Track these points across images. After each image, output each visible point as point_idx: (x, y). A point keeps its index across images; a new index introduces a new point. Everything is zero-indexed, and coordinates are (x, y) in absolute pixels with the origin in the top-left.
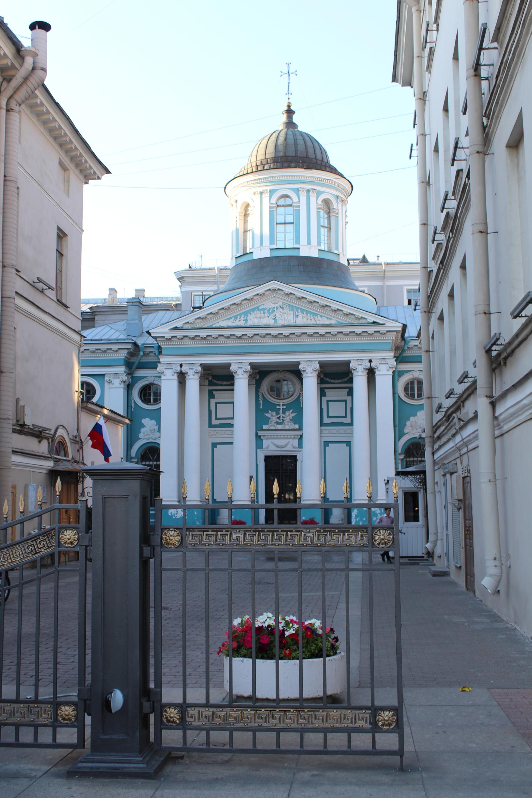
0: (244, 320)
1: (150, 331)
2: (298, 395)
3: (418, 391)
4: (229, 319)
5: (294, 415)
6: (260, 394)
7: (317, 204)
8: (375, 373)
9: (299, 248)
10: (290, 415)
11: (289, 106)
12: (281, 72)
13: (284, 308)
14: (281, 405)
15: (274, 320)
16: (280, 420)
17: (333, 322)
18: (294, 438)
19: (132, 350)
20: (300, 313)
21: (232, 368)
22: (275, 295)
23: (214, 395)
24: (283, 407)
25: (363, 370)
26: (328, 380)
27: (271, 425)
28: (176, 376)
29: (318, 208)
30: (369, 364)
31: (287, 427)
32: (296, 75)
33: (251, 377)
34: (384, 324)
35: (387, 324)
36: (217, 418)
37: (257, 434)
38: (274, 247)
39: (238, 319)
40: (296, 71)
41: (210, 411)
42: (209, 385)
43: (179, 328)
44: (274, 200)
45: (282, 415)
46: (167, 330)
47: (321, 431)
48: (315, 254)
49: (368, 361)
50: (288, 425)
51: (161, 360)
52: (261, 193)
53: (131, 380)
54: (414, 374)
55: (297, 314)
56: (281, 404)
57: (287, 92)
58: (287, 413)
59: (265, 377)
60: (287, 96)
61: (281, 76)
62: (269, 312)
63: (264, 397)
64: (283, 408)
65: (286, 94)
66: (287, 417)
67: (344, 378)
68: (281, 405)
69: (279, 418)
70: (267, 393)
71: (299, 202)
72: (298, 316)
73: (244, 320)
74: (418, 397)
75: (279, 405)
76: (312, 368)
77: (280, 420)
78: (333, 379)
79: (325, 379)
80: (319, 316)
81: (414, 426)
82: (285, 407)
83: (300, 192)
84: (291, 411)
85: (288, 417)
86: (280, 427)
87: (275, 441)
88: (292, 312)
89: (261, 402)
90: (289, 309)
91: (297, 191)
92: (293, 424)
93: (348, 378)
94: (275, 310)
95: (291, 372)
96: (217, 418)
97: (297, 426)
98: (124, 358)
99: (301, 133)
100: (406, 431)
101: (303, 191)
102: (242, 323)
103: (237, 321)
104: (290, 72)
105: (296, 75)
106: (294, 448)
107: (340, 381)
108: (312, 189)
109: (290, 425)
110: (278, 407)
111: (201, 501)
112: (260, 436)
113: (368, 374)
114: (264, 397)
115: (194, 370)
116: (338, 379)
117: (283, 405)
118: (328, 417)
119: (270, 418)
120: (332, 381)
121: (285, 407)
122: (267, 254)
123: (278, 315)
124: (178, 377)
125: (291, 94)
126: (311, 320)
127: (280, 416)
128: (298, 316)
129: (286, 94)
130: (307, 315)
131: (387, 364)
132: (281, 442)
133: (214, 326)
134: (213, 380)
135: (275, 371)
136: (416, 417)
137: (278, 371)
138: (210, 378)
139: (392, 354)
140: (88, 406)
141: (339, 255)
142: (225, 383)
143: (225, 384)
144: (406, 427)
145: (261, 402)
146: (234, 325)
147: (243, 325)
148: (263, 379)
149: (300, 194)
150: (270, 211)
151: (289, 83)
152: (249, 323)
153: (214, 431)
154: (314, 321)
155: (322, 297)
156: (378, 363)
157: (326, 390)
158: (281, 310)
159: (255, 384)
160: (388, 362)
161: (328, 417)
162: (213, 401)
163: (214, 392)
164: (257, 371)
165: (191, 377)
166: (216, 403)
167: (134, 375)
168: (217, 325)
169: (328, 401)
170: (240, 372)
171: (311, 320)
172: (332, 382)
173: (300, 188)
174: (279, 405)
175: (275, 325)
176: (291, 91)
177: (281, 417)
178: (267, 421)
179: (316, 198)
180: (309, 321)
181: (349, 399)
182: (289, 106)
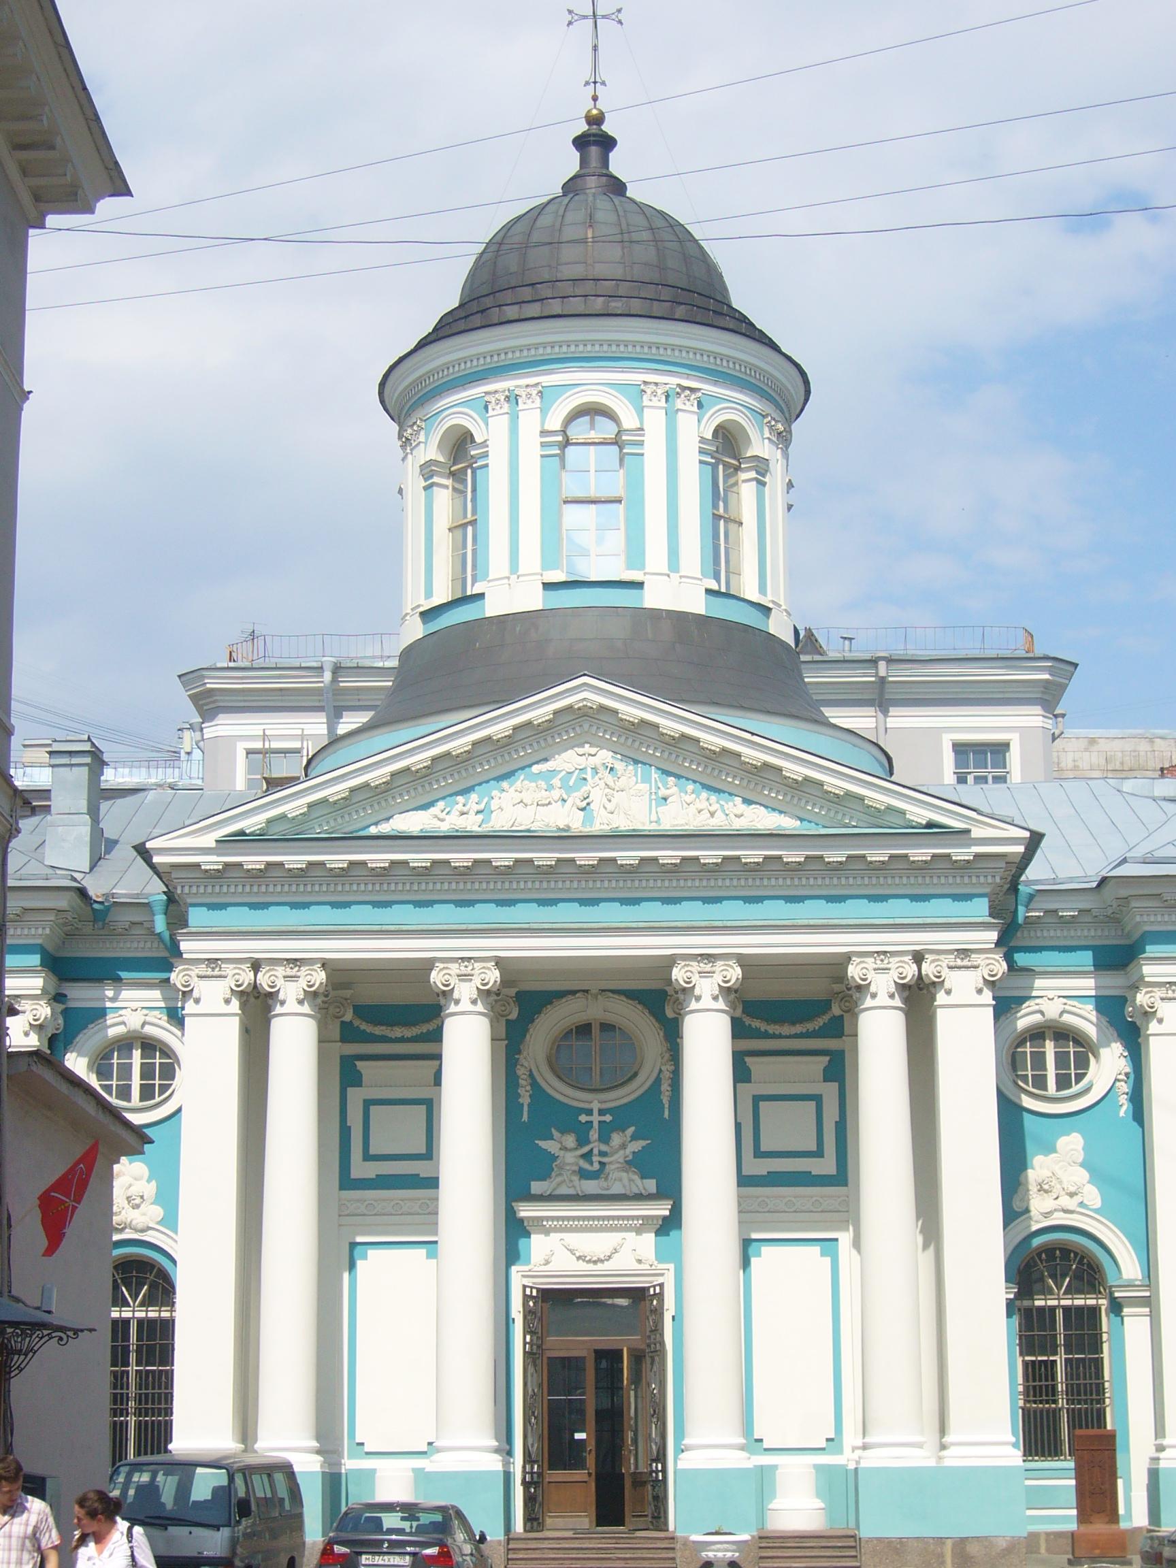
0: (478, 812)
1: (148, 845)
2: (655, 1075)
3: (1058, 1066)
4: (425, 807)
5: (637, 1146)
6: (521, 1071)
7: (703, 440)
8: (933, 998)
9: (639, 585)
10: (626, 1145)
11: (596, 120)
12: (570, 12)
13: (619, 774)
14: (596, 1112)
15: (582, 813)
16: (591, 1164)
17: (787, 823)
18: (639, 1231)
19: (69, 916)
20: (675, 789)
21: (436, 977)
22: (586, 726)
24: (602, 1118)
25: (893, 989)
26: (756, 1024)
27: (559, 1179)
28: (235, 1006)
29: (702, 451)
30: (914, 967)
31: (617, 1189)
32: (620, 22)
33: (496, 1015)
34: (968, 831)
35: (977, 833)
36: (367, 1157)
37: (511, 1214)
38: (558, 576)
39: (460, 807)
40: (619, 11)
41: (345, 1132)
42: (343, 1040)
43: (251, 834)
44: (555, 423)
45: (596, 1147)
46: (209, 840)
47: (739, 1204)
48: (696, 604)
49: (908, 958)
50: (621, 1180)
51: (183, 946)
52: (512, 398)
53: (61, 1021)
54: (1043, 1008)
55: (663, 792)
56: (596, 1106)
57: (587, 75)
58: (616, 1139)
59: (540, 1012)
60: (590, 90)
61: (570, 23)
62: (564, 786)
63: (534, 1084)
64: (599, 1122)
65: (587, 83)
66: (616, 1152)
67: (810, 1018)
68: (596, 1112)
69: (587, 1156)
70: (545, 1069)
71: (642, 429)
72: (665, 799)
73: (478, 812)
74: (1060, 1087)
75: (589, 1112)
76: (718, 978)
77: (591, 1164)
78: (775, 1022)
79: (747, 1021)
80: (738, 800)
81: (1046, 1187)
82: (608, 1118)
83: (645, 397)
84: (632, 1129)
85: (622, 1152)
86: (591, 1187)
87: (573, 1239)
88: (644, 787)
89: (525, 1100)
90: (636, 775)
91: (637, 393)
92: (636, 1178)
93: (826, 1018)
94: (585, 779)
95: (630, 995)
96: (367, 1157)
97: (651, 1185)
98: (39, 941)
99: (642, 208)
101: (654, 394)
102: (471, 824)
103: (455, 812)
104: (599, 12)
105: (620, 22)
106: (639, 1261)
107: (798, 1029)
108: (684, 388)
109: (626, 1181)
110: (583, 1118)
111: (318, 1452)
112: (521, 1220)
113: (906, 1001)
114: (534, 1084)
115: (302, 983)
116: (793, 1023)
117: (602, 1112)
118: (759, 1154)
119: (555, 1158)
120: (771, 1029)
121: (608, 1118)
122: (529, 598)
123: (597, 796)
124: (243, 1006)
125: (603, 83)
126: (712, 814)
127: (592, 1149)
128: (665, 799)
129: (587, 83)
130: (698, 796)
131: (976, 967)
132: (596, 1243)
133: (373, 830)
134: (357, 1023)
135: (573, 993)
136: (1054, 1155)
137: (587, 991)
138: (349, 1016)
139: (993, 936)
140: (34, 1068)
141: (769, 609)
142: (398, 1032)
143: (399, 1035)
145: (525, 1100)
146: (444, 827)
147: (476, 829)
148: (533, 1021)
149: (646, 402)
150: (542, 456)
151: (595, 48)
152: (500, 822)
153: (358, 1201)
154: (724, 817)
155: (753, 734)
156: (944, 965)
157: (747, 1059)
158: (609, 779)
159: (504, 1036)
160: (979, 962)
161: (759, 1154)
162: (355, 1096)
163: (360, 1065)
164: (512, 992)
165: (291, 1006)
166: (368, 1103)
167: (72, 1004)
168: (385, 828)
169: (757, 1099)
170: (465, 992)
171: (712, 814)
172: (771, 1032)
173: (645, 383)
174: (589, 1112)
175: (587, 830)
176: (603, 74)
177: (596, 1151)
178: (545, 1166)
179: (696, 417)
180: (706, 814)
181: (830, 1091)
182: (596, 120)
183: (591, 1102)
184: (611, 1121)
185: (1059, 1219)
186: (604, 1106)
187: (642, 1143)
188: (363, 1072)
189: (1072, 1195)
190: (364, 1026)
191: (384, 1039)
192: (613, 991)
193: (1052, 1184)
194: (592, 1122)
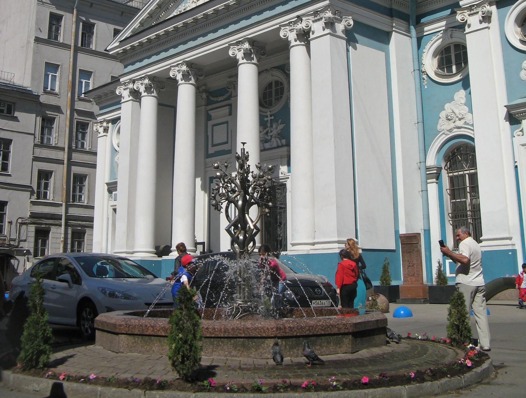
23: (211, 116)
31: (275, 145)
41: (207, 137)
64: (271, 120)
68: (269, 116)
69: (267, 133)
81: (449, 117)
82: (273, 118)
100: (439, 127)
110: (266, 119)
117: (271, 116)
121: (273, 118)
127: (268, 130)
144: (440, 121)
162: (210, 123)
163: (209, 112)
174: (267, 117)
177: (269, 131)
183: (267, 112)
184: (274, 119)
185: (457, 132)
186: (272, 113)
187: (283, 125)
188: (211, 115)
189: (460, 119)
190: (213, 99)
191: (217, 102)
192: (274, 68)
193: (452, 116)
194: (268, 120)
